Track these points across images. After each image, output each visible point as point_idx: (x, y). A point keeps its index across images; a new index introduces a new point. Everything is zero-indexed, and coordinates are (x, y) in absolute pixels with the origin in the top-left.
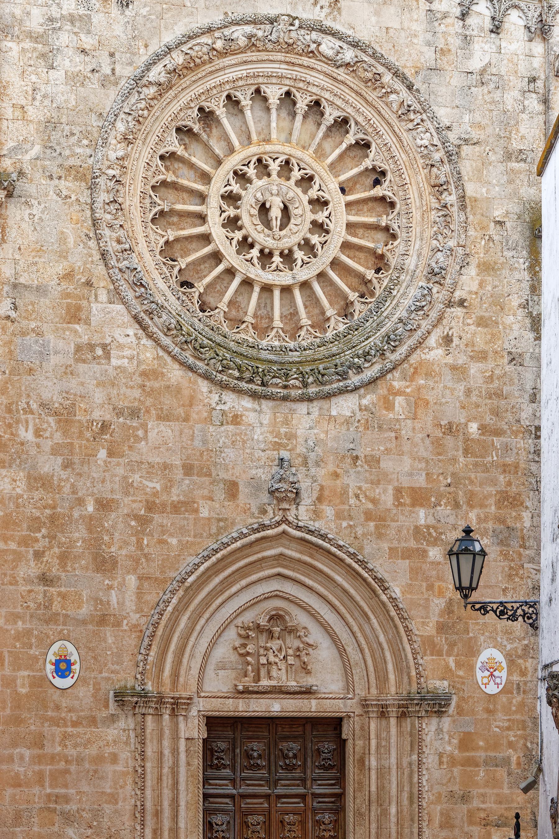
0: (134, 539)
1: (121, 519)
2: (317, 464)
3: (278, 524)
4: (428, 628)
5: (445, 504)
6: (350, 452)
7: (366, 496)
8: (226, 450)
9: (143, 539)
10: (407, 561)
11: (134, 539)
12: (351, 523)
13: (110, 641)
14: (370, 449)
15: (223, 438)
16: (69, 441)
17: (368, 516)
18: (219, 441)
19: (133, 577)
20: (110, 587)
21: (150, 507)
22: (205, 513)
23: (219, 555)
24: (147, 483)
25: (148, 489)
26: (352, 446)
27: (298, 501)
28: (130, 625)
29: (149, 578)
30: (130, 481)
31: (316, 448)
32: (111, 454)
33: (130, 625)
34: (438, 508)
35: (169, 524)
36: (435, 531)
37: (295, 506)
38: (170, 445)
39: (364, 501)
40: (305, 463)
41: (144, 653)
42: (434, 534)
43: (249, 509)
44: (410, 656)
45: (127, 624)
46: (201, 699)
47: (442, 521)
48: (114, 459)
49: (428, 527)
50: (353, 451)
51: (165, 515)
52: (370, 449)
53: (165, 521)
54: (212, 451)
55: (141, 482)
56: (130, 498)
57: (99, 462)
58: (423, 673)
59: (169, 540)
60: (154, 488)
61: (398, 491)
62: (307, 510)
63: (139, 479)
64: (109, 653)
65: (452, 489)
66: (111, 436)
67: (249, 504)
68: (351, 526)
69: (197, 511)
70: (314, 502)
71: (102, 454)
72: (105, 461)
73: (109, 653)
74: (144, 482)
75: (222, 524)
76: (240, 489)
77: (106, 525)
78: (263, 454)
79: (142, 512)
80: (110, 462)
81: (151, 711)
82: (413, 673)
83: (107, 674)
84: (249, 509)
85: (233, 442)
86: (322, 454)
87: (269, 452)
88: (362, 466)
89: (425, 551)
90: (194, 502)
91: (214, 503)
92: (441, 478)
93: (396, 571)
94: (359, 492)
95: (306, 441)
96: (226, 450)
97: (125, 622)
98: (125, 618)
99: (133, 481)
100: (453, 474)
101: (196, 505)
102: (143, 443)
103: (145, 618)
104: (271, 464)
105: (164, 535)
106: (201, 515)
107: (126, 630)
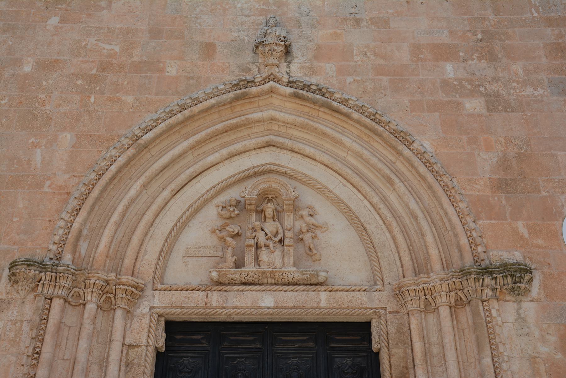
0: (77, 97)
1: (65, 78)
2: (313, 26)
3: (265, 81)
4: (478, 187)
5: (478, 57)
6: (352, 15)
7: (376, 54)
8: (202, 17)
9: (90, 97)
10: (437, 114)
11: (77, 97)
12: (358, 78)
13: (21, 206)
14: (377, 12)
15: (201, 7)
16: (15, 9)
17: (379, 71)
18: (195, 9)
19: (69, 136)
20: (35, 145)
21: (104, 67)
22: (172, 70)
23: (187, 113)
24: (104, 46)
25: (105, 51)
26: (354, 10)
27: (289, 59)
28: (53, 186)
29: (91, 136)
30: (84, 43)
31: (311, 13)
32: (63, 21)
33: (53, 186)
34: (470, 62)
35: (126, 83)
36: (469, 84)
37: (285, 64)
38: (137, 13)
39: (372, 58)
40: (298, 24)
41: (66, 218)
42: (469, 87)
43: (229, 67)
44: (456, 220)
45: (50, 186)
46: (157, 292)
47: (477, 73)
48: (67, 25)
49: (460, 81)
50: (356, 15)
51: (122, 74)
52: (377, 12)
53: (120, 80)
54: (187, 17)
55: (96, 45)
56: (81, 59)
57: (48, 28)
58: (478, 240)
59: (123, 98)
60: (112, 50)
61: (416, 49)
62: (302, 67)
63: (94, 42)
64: (15, 220)
65: (484, 44)
66: (68, 5)
67: (229, 63)
68: (357, 81)
69: (163, 70)
70: (311, 60)
71: (54, 21)
72: (56, 27)
73: (15, 220)
74: (101, 44)
75: (192, 82)
76: (218, 49)
77: (45, 83)
78: (247, 19)
79: (94, 72)
80: (62, 27)
81: (60, 292)
82: (464, 241)
83: (6, 246)
84: (229, 67)
85: (213, 10)
86: (318, 18)
87: (255, 18)
88: (367, 27)
89: (459, 106)
90: (160, 62)
91: (184, 62)
92: (469, 35)
93: (422, 125)
94: (366, 50)
95: (299, 7)
96: (202, 17)
97: (48, 183)
98: (49, 178)
99: (87, 44)
100: (482, 32)
101: (162, 65)
102: (105, 11)
103: (77, 179)
104: (256, 27)
105: (117, 93)
106: (168, 74)
107: (46, 193)
